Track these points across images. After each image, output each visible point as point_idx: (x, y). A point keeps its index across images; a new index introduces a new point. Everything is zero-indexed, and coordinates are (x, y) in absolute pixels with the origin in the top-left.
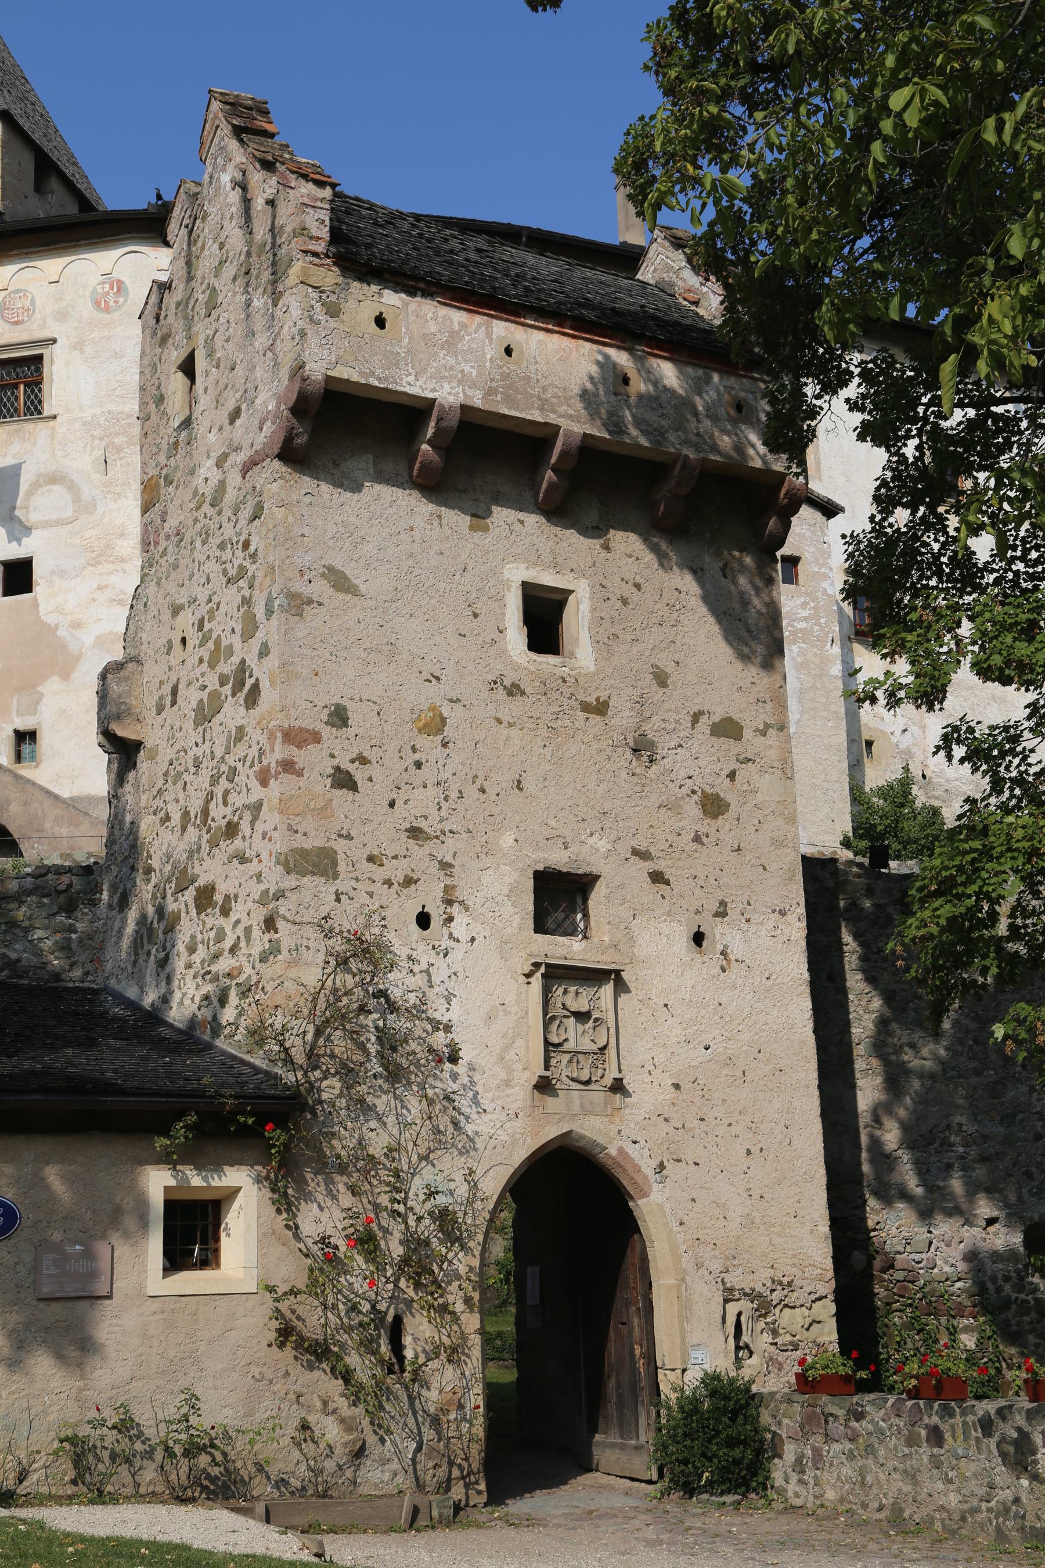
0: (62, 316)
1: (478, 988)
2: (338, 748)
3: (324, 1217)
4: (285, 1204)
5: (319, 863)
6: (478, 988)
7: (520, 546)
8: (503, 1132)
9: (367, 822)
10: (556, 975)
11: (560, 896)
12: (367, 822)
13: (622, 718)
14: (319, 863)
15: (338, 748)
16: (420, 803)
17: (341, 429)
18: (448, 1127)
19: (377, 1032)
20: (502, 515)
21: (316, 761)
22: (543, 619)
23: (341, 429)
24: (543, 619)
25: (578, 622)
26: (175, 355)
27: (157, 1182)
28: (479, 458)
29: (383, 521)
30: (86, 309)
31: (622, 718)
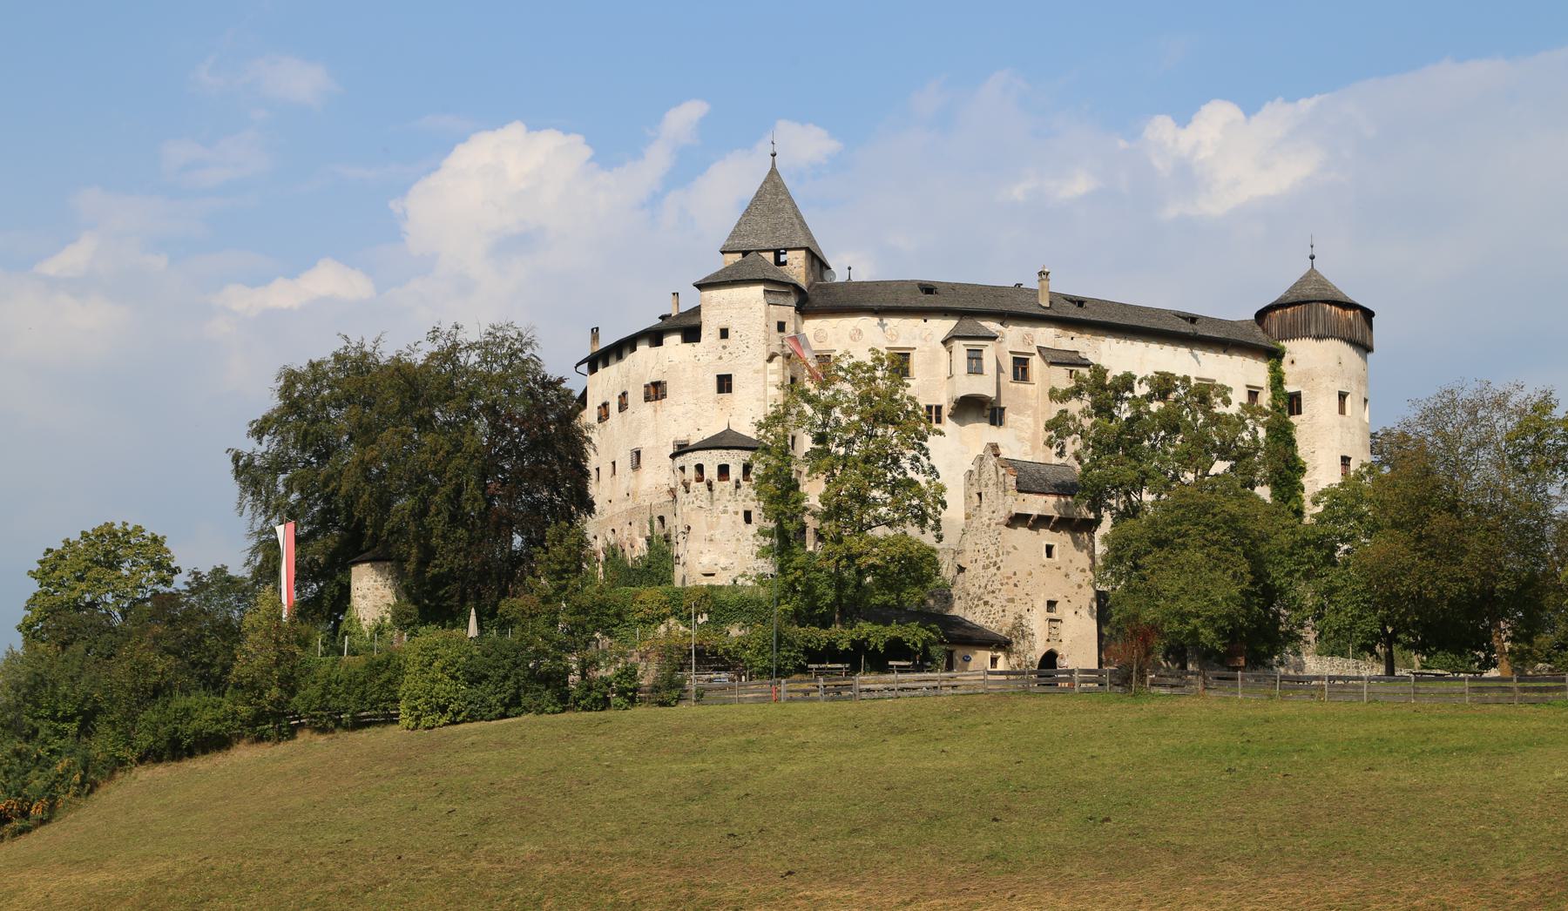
0: (838, 341)
1: (1037, 622)
2: (1014, 580)
3: (1014, 661)
4: (1008, 658)
5: (1012, 600)
6: (1037, 622)
7: (1046, 536)
8: (1040, 649)
9: (1019, 593)
10: (1051, 620)
11: (1051, 605)
12: (1019, 593)
13: (1063, 570)
14: (1012, 600)
15: (1014, 580)
16: (1028, 589)
17: (1017, 520)
18: (1031, 648)
19: (1020, 630)
20: (1042, 531)
21: (1011, 582)
22: (1049, 549)
23: (1017, 520)
24: (1049, 549)
25: (1055, 551)
26: (975, 490)
27: (989, 654)
28: (1041, 522)
29: (1022, 532)
30: (848, 340)
31: (1063, 570)
